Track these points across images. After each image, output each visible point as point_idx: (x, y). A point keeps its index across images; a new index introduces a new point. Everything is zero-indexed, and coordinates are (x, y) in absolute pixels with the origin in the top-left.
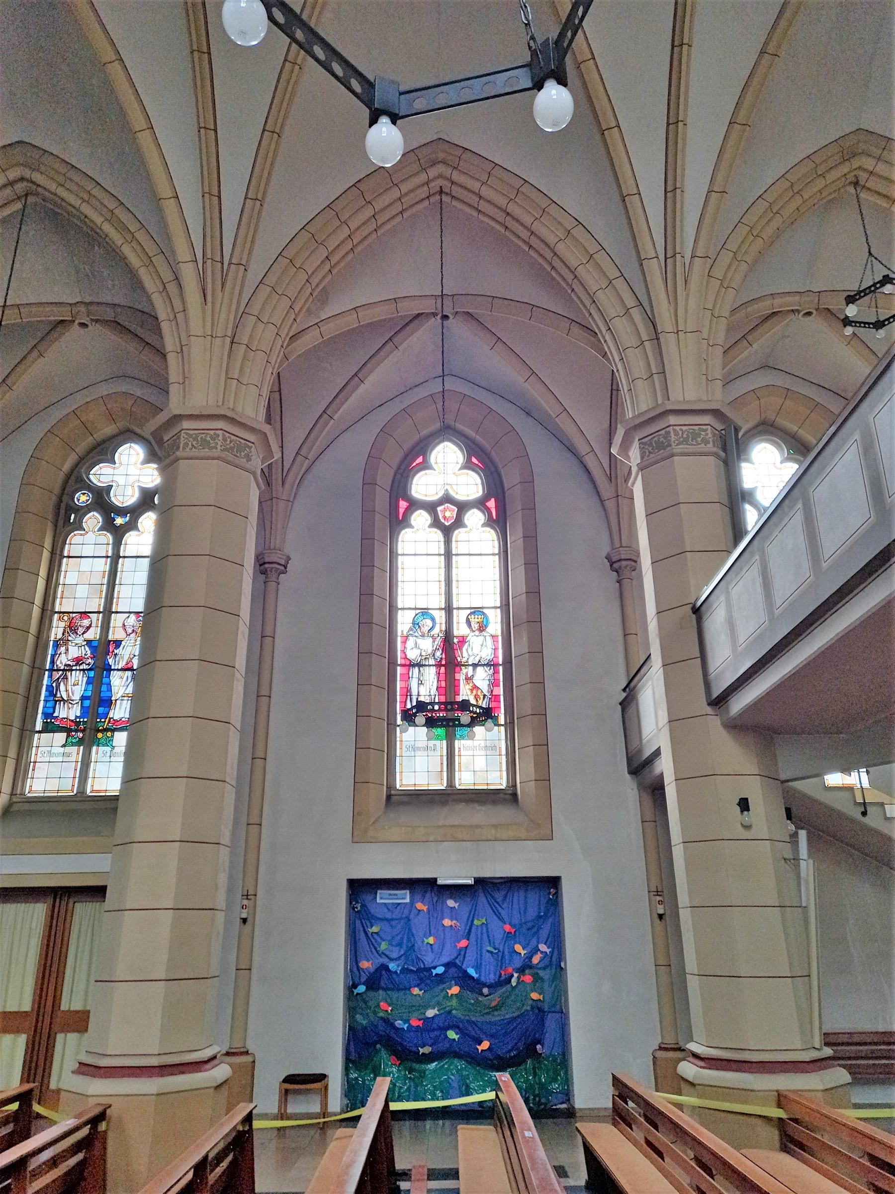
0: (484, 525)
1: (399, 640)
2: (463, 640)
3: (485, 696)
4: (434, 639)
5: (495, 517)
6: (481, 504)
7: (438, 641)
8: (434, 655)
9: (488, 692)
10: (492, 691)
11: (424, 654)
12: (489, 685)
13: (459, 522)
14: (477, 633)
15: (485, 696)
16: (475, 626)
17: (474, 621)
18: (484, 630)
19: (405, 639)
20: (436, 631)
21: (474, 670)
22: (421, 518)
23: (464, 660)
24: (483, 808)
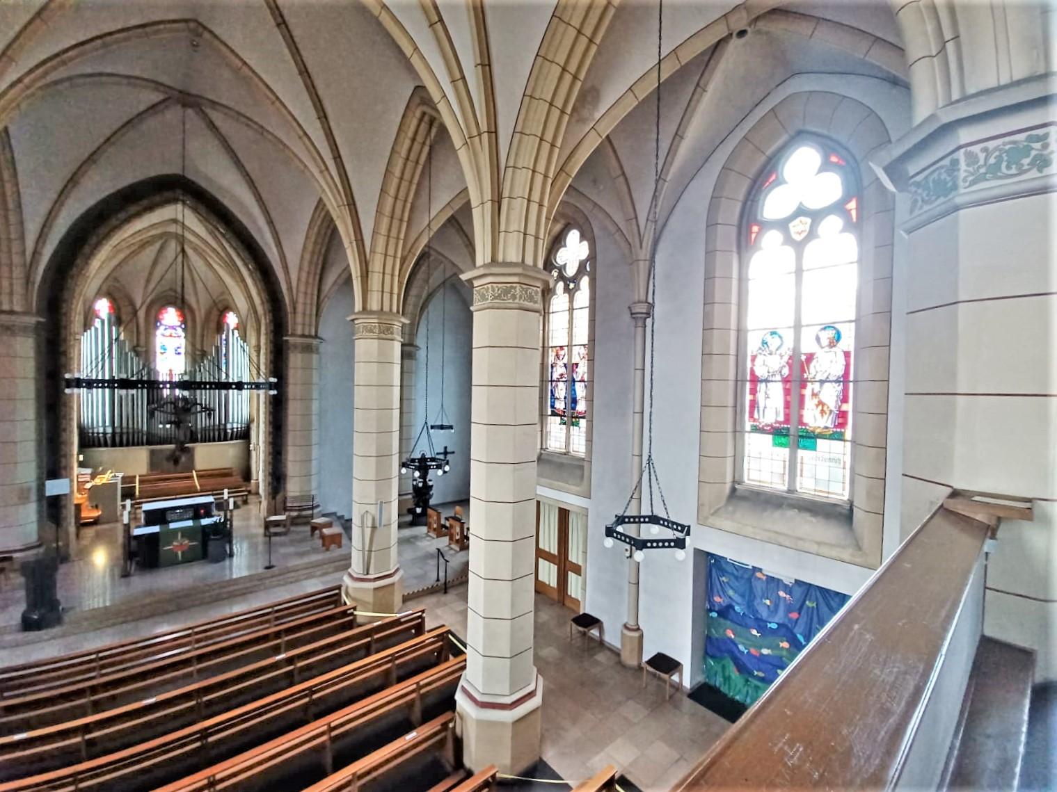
0: (844, 230)
1: (749, 359)
2: (810, 358)
3: (831, 411)
4: (782, 357)
5: (854, 220)
6: (838, 208)
7: (786, 358)
8: (780, 372)
9: (836, 407)
10: (840, 407)
11: (771, 371)
12: (837, 401)
13: (812, 234)
14: (827, 349)
15: (831, 411)
16: (825, 342)
17: (826, 336)
18: (834, 346)
19: (754, 358)
20: (783, 350)
21: (821, 386)
22: (771, 240)
23: (811, 376)
24: (813, 520)
